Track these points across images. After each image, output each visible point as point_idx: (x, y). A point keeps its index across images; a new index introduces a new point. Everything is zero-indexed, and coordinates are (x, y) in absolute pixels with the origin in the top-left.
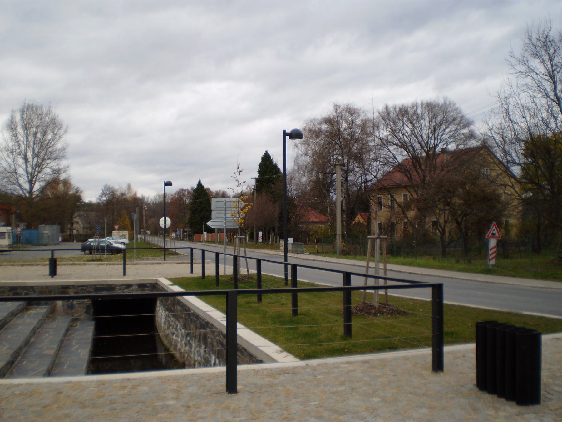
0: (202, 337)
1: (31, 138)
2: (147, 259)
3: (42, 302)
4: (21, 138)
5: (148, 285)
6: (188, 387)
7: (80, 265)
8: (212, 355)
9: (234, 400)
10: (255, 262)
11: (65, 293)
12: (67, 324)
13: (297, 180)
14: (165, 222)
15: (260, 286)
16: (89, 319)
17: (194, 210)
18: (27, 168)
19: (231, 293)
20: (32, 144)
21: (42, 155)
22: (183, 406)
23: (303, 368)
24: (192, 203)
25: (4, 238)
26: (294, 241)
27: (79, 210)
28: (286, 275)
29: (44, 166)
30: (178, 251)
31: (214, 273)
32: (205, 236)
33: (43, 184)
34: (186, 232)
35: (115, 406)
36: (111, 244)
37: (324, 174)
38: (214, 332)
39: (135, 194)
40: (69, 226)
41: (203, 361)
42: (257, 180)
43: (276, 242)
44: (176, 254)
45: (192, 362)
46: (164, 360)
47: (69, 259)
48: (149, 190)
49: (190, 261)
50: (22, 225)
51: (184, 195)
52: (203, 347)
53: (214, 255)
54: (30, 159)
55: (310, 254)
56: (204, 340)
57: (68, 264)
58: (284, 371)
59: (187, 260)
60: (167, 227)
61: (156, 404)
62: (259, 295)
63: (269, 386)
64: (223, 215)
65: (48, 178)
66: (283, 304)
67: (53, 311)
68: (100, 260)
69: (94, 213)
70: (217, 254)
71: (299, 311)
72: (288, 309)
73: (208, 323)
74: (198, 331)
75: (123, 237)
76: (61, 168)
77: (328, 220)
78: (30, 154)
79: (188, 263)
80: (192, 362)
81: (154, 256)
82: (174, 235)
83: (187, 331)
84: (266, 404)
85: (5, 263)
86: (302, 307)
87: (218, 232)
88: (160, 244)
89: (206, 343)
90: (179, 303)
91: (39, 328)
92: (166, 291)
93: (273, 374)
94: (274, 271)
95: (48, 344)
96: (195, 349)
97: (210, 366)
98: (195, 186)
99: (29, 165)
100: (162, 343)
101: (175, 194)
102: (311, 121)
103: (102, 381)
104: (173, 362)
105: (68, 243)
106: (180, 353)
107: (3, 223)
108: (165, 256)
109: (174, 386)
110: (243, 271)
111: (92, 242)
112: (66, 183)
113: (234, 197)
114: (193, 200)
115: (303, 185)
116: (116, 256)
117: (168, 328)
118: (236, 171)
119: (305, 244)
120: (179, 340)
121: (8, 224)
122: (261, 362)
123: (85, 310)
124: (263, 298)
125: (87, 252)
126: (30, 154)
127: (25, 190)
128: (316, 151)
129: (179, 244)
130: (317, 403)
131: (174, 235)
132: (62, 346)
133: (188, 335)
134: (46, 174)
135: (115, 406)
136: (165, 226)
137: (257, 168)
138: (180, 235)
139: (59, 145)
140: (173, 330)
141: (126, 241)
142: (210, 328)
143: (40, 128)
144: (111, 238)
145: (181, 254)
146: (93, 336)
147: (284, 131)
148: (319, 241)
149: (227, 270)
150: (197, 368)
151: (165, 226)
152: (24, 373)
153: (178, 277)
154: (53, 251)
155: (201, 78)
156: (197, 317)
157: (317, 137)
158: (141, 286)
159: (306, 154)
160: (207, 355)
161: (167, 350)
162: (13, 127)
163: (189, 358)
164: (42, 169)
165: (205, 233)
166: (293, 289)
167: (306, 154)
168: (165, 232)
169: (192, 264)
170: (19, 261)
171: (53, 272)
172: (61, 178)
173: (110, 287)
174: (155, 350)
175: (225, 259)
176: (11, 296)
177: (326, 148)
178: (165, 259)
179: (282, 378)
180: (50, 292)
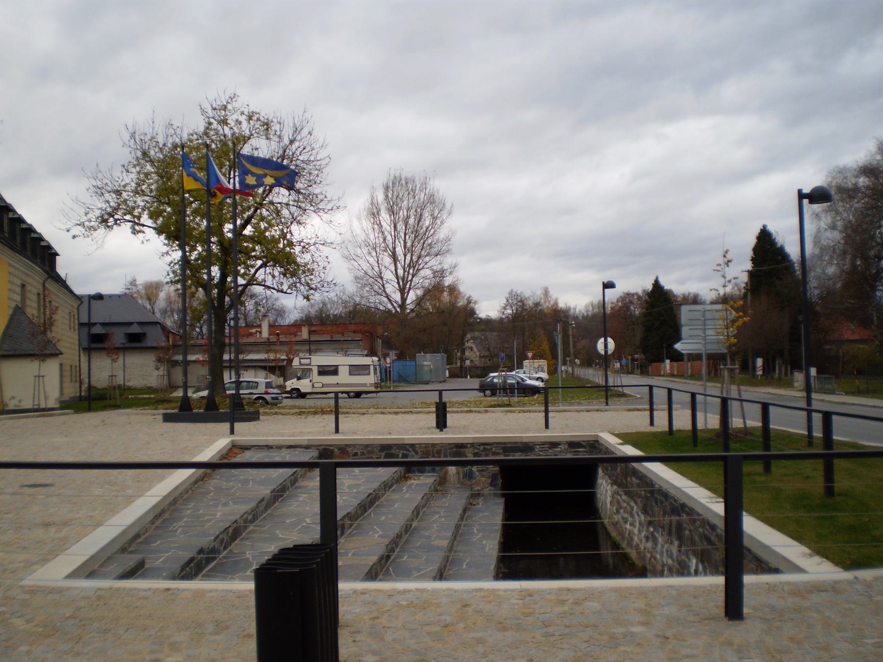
0: (674, 530)
1: (401, 226)
2: (579, 404)
3: (427, 468)
4: (387, 225)
5: (584, 444)
6: (663, 606)
7: (479, 412)
8: (691, 557)
9: (736, 631)
10: (758, 408)
11: (460, 456)
12: (464, 501)
13: (818, 270)
14: (605, 345)
15: (767, 447)
16: (495, 495)
17: (650, 325)
18: (396, 270)
19: (728, 458)
20: (402, 235)
21: (417, 249)
22: (658, 636)
23: (848, 582)
24: (645, 315)
25: (369, 374)
26: (818, 373)
27: (472, 331)
28: (810, 428)
29: (421, 266)
30: (626, 391)
31: (689, 427)
32: (668, 367)
33: (420, 292)
34: (636, 360)
35: (551, 630)
36: (523, 380)
37: (865, 258)
38: (695, 521)
39: (556, 303)
40: (459, 354)
41: (676, 566)
42: (751, 274)
43: (786, 375)
44: (623, 395)
45: (659, 567)
46: (611, 561)
47: (461, 404)
48: (578, 296)
49: (648, 407)
50: (393, 355)
51: (631, 302)
52: (676, 543)
53: (687, 398)
54: (401, 257)
55: (847, 393)
56: (677, 532)
57: (462, 412)
58: (818, 588)
59: (642, 404)
60: (610, 352)
61: (615, 631)
62: (767, 462)
63: (795, 610)
64: (700, 333)
65: (427, 283)
66: (807, 477)
67: (443, 481)
68: (509, 405)
69: (495, 334)
70: (693, 395)
71: (836, 489)
72: (817, 485)
73: (683, 506)
74: (667, 518)
75: (539, 369)
76: (445, 268)
77: (875, 337)
78: (399, 250)
79: (645, 410)
80: (659, 567)
81: (588, 399)
82: (618, 365)
83: (649, 518)
84: (792, 639)
85: (372, 410)
86: (842, 482)
87: (689, 360)
88: (597, 380)
89: (680, 538)
90: (635, 473)
91: (423, 507)
92: (613, 453)
93: (798, 591)
94: (788, 423)
95: (437, 530)
96: (663, 546)
97: (689, 574)
98: (650, 287)
99: (399, 266)
100: (608, 534)
101: (618, 301)
102: (840, 172)
103: (528, 590)
104: (625, 566)
105: (460, 379)
106: (638, 553)
107: (365, 352)
108: (607, 399)
109: (640, 604)
110: (736, 422)
111: (494, 377)
112: (453, 289)
113: (712, 303)
114: (647, 309)
115: (830, 279)
116: (531, 398)
117: (618, 512)
118: (721, 260)
119: (836, 378)
120: (636, 531)
121: (372, 353)
122: (776, 571)
123: (490, 480)
124: (773, 468)
125: (488, 392)
126: (399, 250)
127: (396, 302)
128: (850, 222)
129: (627, 380)
130: (877, 640)
131: (618, 365)
132: (458, 534)
133: (650, 523)
134: (424, 277)
135: (551, 630)
136: (606, 352)
137: (750, 253)
138: (627, 365)
139: (442, 234)
140: (626, 515)
141: (544, 375)
142: (688, 514)
143: (413, 210)
144: (522, 371)
145: (631, 396)
146: (503, 520)
147: (800, 191)
148: (860, 372)
149: (710, 421)
150: (667, 577)
151: (606, 352)
152: (405, 574)
153: (629, 431)
154: (441, 392)
155: (670, 115)
156: (666, 495)
157: (851, 197)
158: (574, 445)
159: (833, 227)
160: (684, 557)
161: (616, 546)
162: (375, 210)
163: (653, 560)
164: (418, 270)
165: (668, 361)
166: (828, 454)
167: (833, 227)
168: (605, 361)
169: (652, 410)
170: (391, 408)
171: (441, 424)
172: (447, 284)
173: (526, 447)
174: (596, 546)
175: (705, 403)
176: (382, 460)
177: (868, 215)
178: (607, 404)
179: (815, 598)
180: (439, 453)
